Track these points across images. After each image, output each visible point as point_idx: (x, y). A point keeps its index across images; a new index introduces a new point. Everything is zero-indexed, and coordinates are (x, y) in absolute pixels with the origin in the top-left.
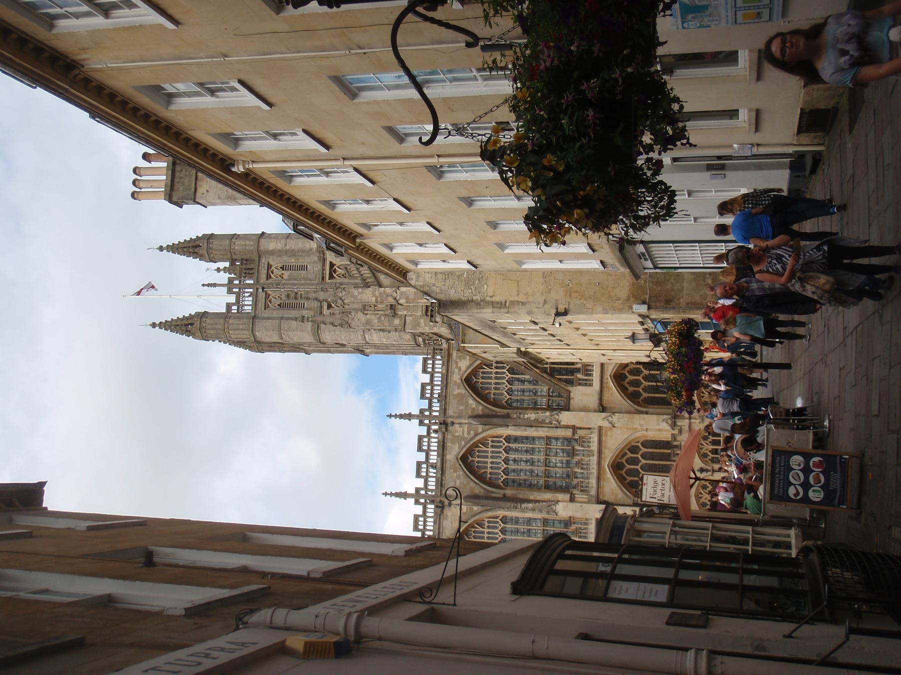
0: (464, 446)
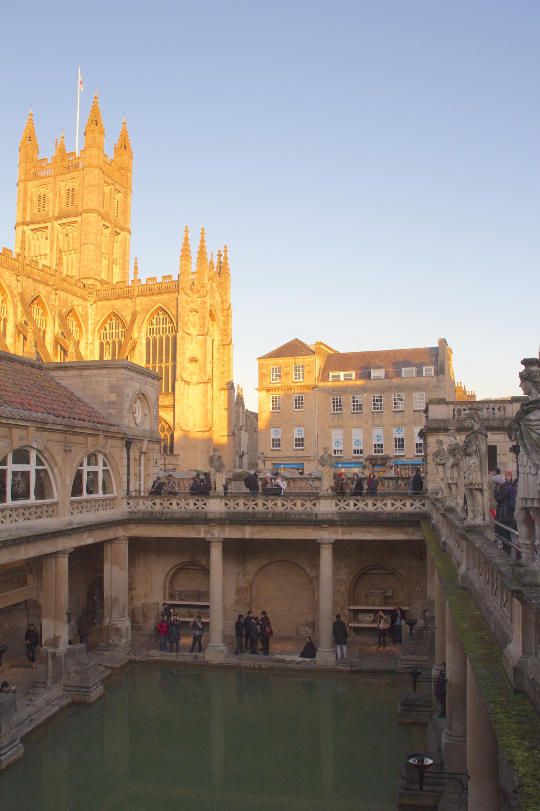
0: (46, 300)
